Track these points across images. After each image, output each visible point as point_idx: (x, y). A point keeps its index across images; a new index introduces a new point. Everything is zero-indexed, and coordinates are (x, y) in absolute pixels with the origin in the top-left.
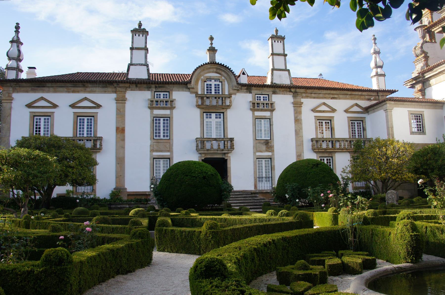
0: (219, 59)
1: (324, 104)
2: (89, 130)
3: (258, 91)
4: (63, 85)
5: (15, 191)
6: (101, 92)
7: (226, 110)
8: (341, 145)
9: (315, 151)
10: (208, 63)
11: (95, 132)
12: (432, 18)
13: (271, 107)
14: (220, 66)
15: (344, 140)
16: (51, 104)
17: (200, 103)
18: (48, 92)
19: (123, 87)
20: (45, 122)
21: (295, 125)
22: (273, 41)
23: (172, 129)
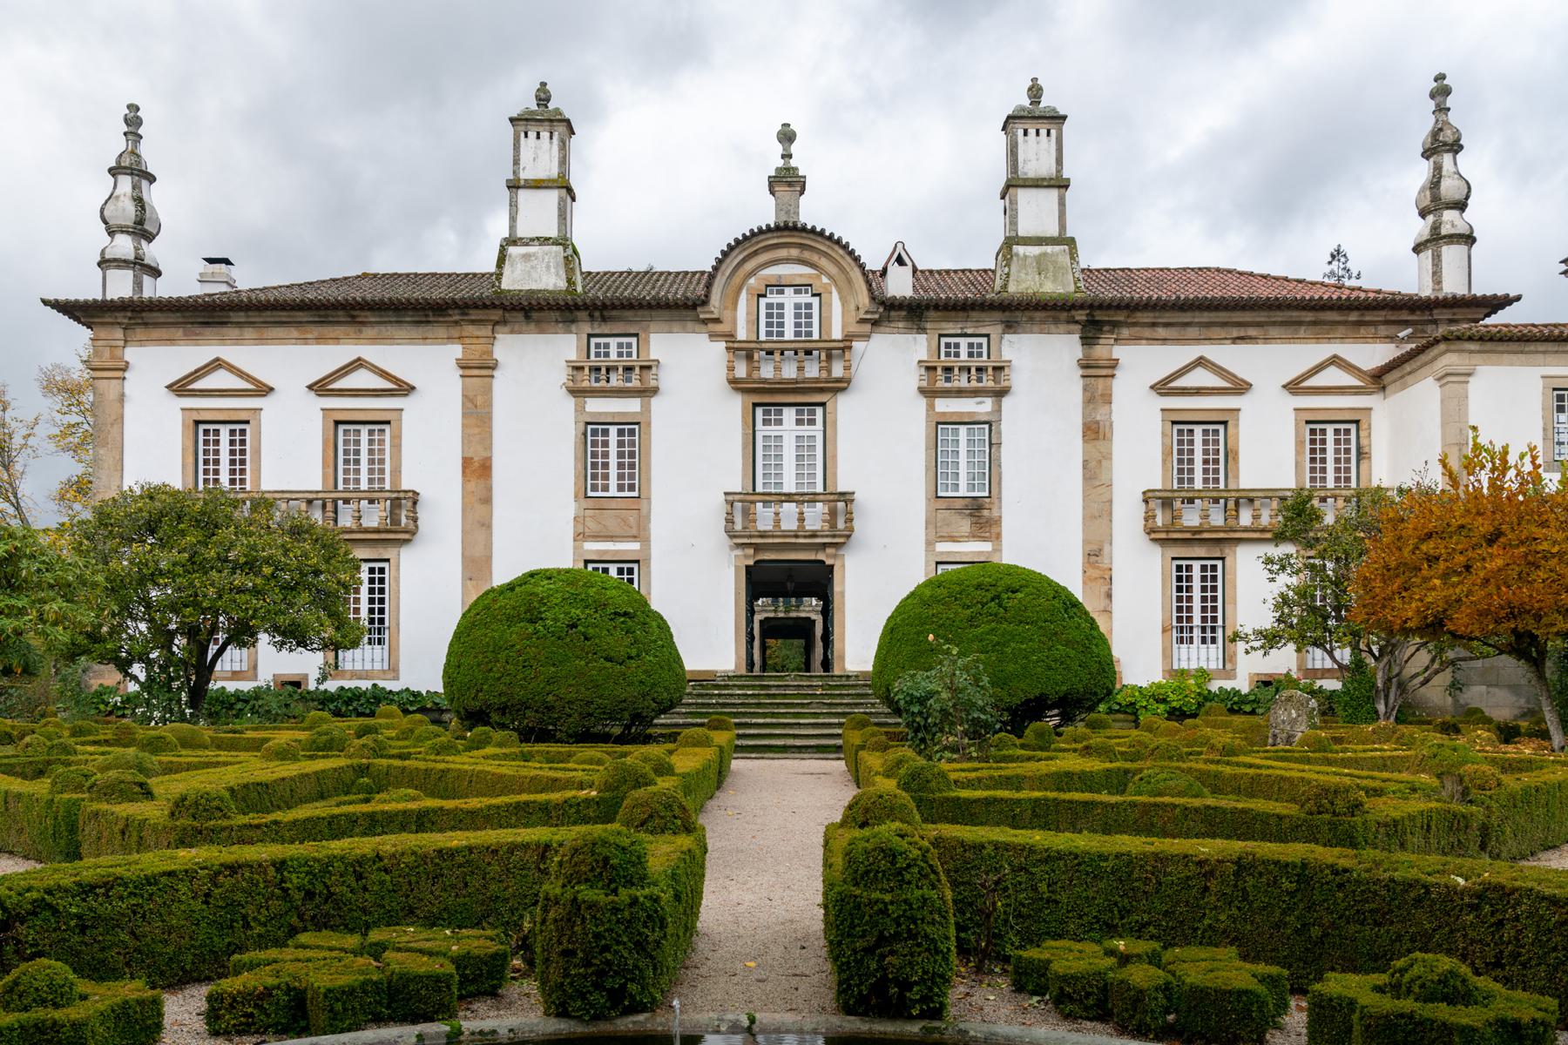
0: (810, 212)
4: (284, 319)
6: (411, 340)
9: (1153, 536)
11: (397, 472)
14: (811, 236)
18: (238, 341)
19: (481, 321)
20: (232, 443)
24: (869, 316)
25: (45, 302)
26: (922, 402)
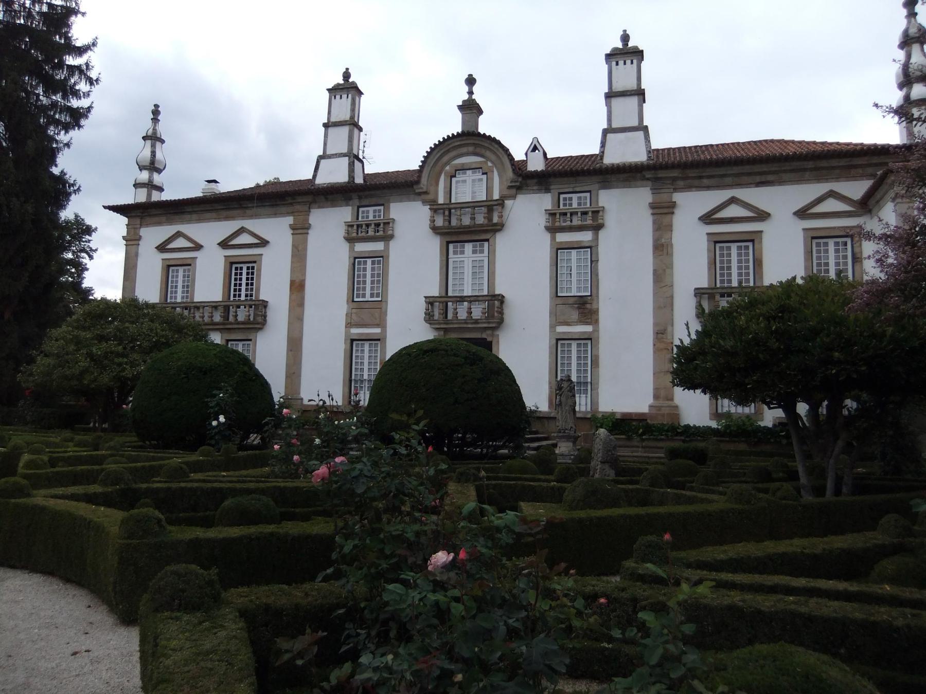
3: (566, 186)
6: (269, 216)
7: (492, 234)
17: (440, 222)
18: (189, 221)
21: (654, 257)
24: (513, 184)
25: (105, 207)
26: (548, 236)
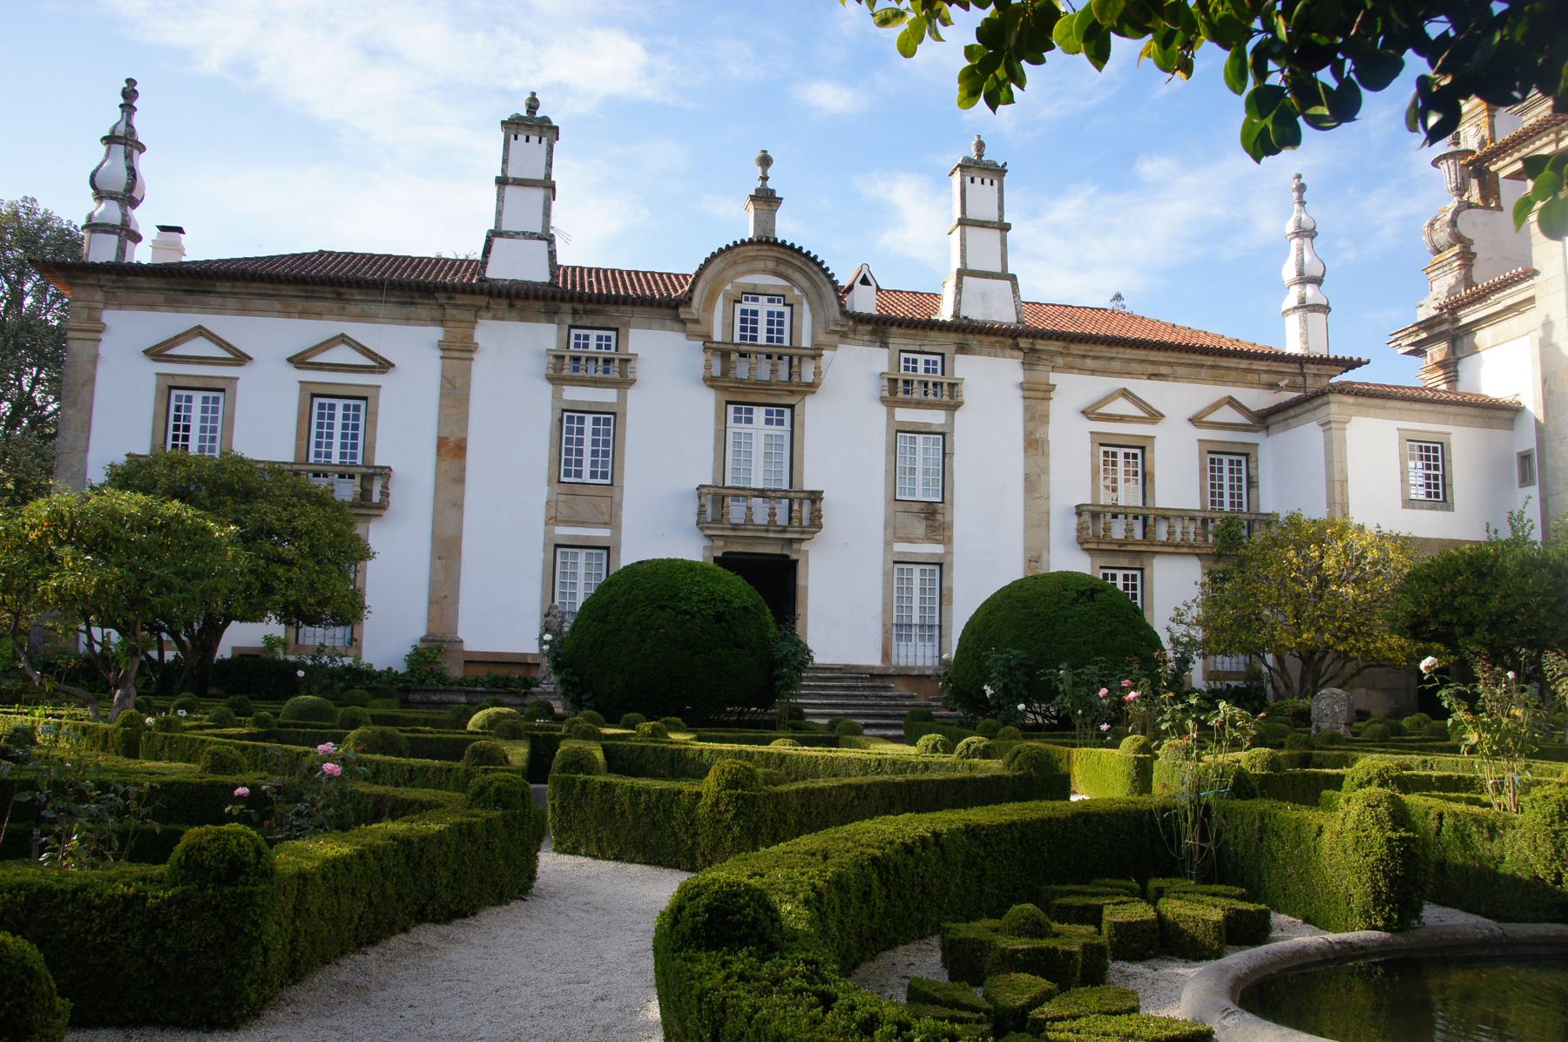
0: (787, 229)
1: (1125, 393)
2: (349, 441)
3: (910, 341)
5: (97, 632)
6: (394, 320)
7: (799, 398)
8: (1174, 532)
9: (1086, 546)
10: (751, 240)
11: (369, 448)
12: (1492, 127)
13: (948, 396)
14: (789, 252)
15: (1182, 514)
16: (226, 350)
17: (716, 370)
18: (221, 310)
19: (466, 306)
20: (205, 410)
21: (1026, 457)
22: (968, 179)
23: (623, 454)
24: (839, 329)
